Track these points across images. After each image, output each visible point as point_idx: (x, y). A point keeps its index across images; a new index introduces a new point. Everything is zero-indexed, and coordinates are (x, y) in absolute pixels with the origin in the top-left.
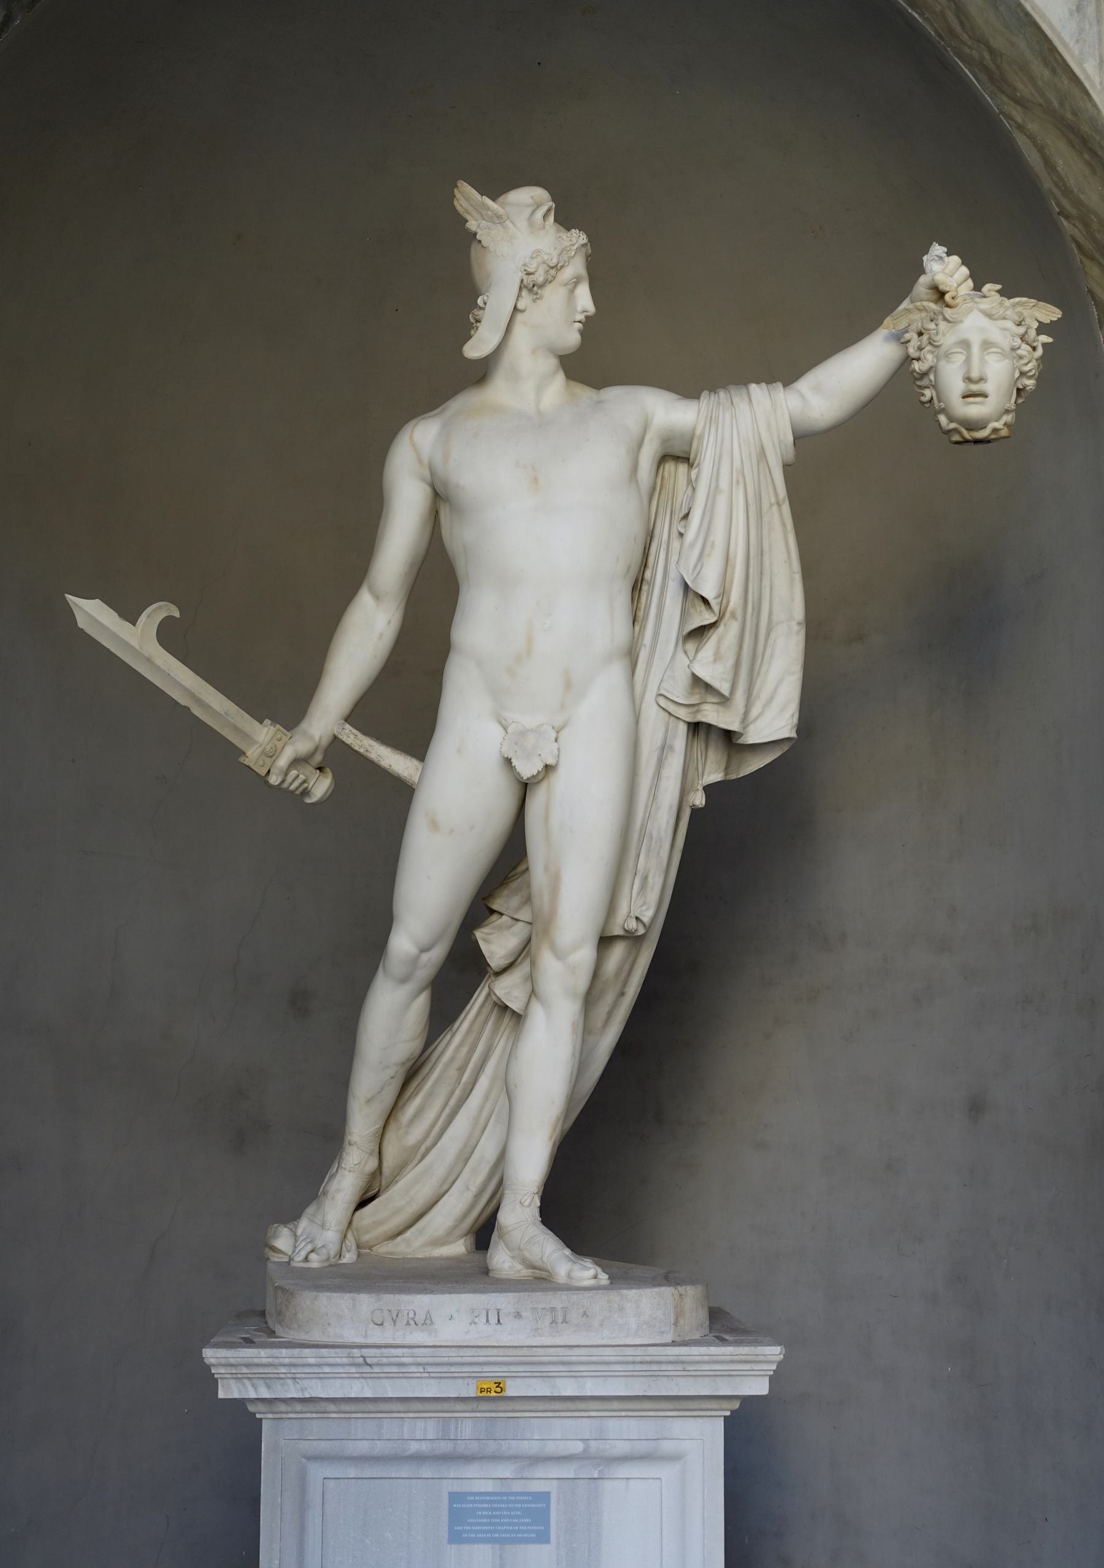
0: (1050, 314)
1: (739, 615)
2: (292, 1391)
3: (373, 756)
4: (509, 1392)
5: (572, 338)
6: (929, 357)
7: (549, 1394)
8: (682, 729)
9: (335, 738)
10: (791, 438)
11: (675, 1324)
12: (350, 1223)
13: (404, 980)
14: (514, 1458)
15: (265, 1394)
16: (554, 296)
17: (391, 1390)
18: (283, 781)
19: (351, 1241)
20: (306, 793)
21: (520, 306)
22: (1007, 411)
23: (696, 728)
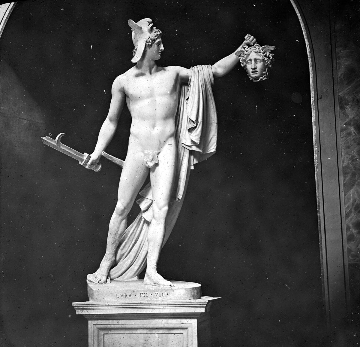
16: (155, 47)
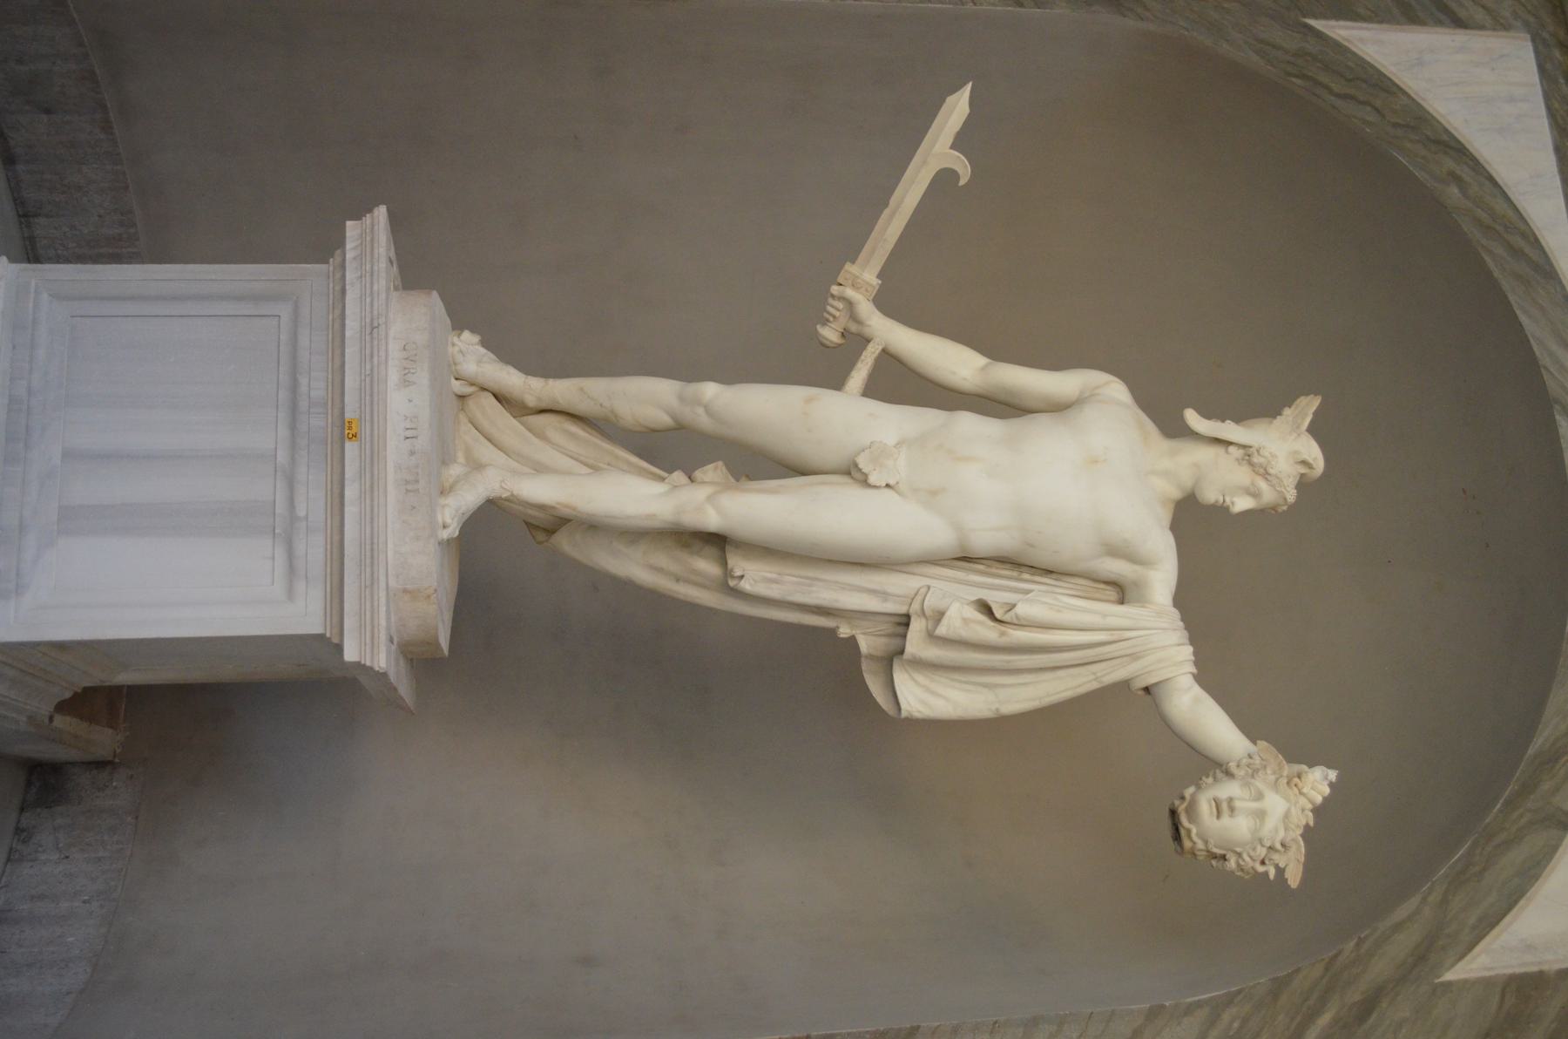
0: (1294, 878)
1: (1004, 641)
2: (349, 276)
3: (859, 365)
4: (348, 445)
5: (1210, 495)
6: (1242, 773)
7: (347, 476)
8: (903, 610)
9: (868, 341)
10: (1151, 680)
11: (405, 591)
12: (484, 389)
13: (681, 398)
14: (293, 460)
15: (349, 256)
16: (1243, 476)
17: (351, 351)
18: (833, 296)
19: (468, 390)
20: (825, 322)
21: (1231, 449)
22: (1206, 842)
23: (904, 621)
